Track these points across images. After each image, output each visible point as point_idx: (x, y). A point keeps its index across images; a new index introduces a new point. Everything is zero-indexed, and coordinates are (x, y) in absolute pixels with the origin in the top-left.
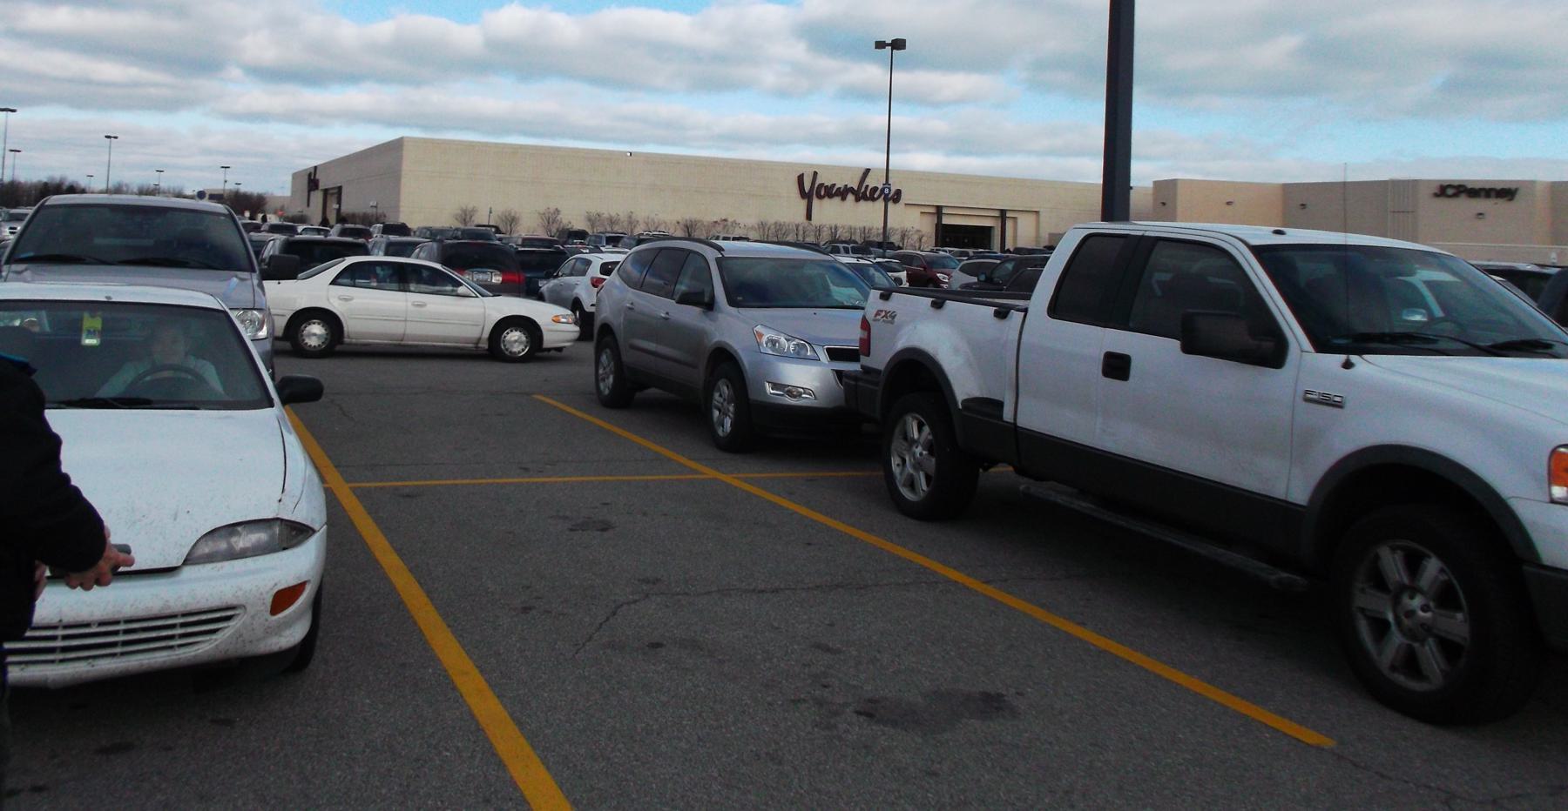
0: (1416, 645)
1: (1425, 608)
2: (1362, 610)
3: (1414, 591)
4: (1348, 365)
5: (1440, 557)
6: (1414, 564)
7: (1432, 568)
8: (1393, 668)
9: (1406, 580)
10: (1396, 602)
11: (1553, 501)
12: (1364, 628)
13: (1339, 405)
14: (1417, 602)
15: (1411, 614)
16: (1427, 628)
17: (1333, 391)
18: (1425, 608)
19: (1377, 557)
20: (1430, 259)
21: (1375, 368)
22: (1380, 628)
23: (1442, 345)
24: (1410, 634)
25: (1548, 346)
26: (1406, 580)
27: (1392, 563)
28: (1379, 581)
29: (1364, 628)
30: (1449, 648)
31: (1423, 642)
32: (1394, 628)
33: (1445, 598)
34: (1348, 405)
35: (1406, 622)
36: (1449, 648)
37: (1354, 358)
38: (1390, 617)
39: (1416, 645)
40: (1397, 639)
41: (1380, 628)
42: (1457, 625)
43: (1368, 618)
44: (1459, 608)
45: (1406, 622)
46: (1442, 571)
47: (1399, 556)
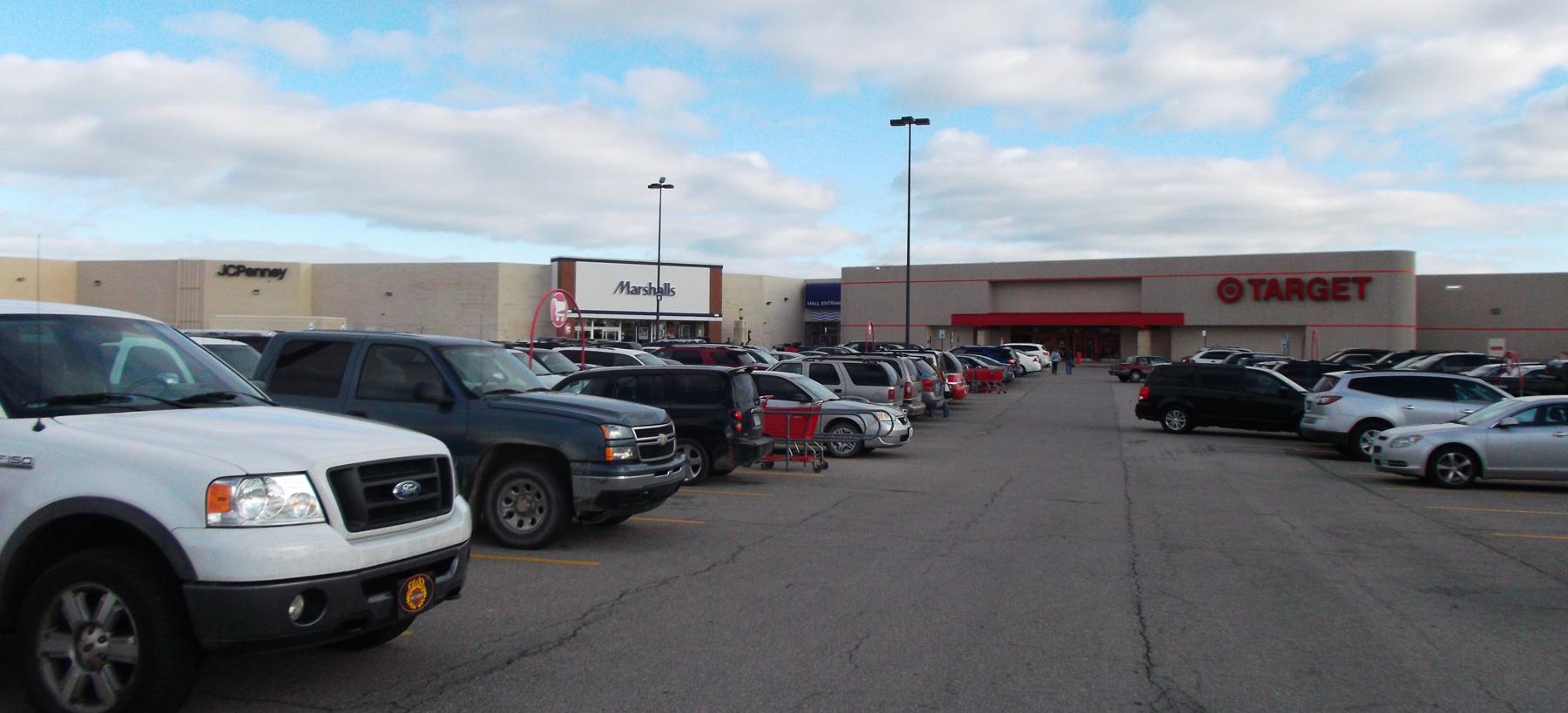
0: (93, 674)
1: (102, 639)
2: (46, 654)
3: (92, 626)
4: (39, 428)
5: (116, 592)
6: (93, 602)
7: (109, 601)
8: (73, 700)
9: (86, 618)
10: (77, 639)
11: (208, 527)
12: (47, 670)
13: (28, 467)
14: (96, 634)
15: (89, 647)
16: (103, 657)
17: (22, 454)
18: (102, 639)
19: (61, 603)
20: (138, 327)
21: (67, 429)
22: (62, 666)
23: (136, 401)
24: (91, 666)
25: (233, 397)
26: (86, 618)
27: (74, 605)
28: (62, 625)
29: (47, 670)
30: (122, 670)
31: (99, 670)
32: (74, 664)
33: (120, 627)
34: (37, 465)
35: (86, 655)
36: (122, 670)
37: (45, 421)
38: (72, 654)
39: (93, 674)
40: (77, 673)
41: (62, 666)
42: (129, 647)
43: (51, 660)
44: (129, 633)
45: (86, 655)
46: (117, 603)
47: (80, 597)
